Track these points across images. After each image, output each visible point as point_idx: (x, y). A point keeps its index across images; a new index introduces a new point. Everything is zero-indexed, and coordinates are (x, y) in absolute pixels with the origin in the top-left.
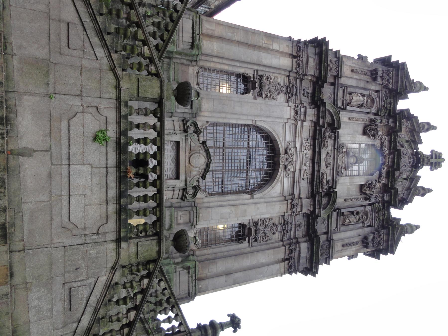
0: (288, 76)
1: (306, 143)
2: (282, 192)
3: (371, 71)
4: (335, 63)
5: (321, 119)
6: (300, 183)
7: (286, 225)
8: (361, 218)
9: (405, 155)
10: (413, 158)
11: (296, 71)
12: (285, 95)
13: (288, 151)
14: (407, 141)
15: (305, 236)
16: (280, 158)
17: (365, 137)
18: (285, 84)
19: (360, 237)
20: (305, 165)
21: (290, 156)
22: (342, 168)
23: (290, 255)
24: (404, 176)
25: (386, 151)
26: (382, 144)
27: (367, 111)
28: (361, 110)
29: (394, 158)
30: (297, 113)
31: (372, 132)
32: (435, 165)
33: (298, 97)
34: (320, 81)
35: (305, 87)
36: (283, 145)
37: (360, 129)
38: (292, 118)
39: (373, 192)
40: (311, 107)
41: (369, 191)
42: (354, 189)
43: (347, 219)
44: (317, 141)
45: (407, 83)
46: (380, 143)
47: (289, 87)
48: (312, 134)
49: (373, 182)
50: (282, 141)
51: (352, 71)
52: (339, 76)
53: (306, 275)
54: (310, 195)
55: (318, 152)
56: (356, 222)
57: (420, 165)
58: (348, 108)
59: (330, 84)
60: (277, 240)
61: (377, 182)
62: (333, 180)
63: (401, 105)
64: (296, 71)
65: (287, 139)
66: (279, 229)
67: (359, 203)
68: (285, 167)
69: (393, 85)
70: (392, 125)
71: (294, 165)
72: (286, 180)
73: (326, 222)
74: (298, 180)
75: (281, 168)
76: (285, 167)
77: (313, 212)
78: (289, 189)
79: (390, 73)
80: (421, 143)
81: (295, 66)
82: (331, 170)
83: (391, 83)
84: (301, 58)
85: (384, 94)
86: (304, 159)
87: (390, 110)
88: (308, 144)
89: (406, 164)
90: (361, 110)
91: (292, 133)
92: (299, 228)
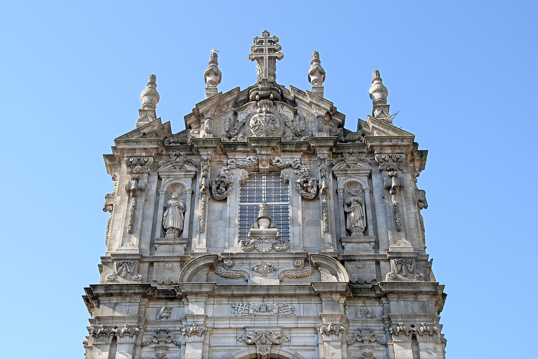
0: (142, 346)
1: (239, 310)
2: (312, 348)
3: (129, 196)
4: (121, 265)
5: (203, 290)
6: (298, 318)
7: (363, 339)
8: (357, 198)
9: (256, 123)
10: (261, 107)
11: (135, 337)
12: (171, 349)
13: (250, 341)
14: (236, 114)
15: (381, 302)
16: (261, 353)
17: (228, 200)
18: (153, 349)
19: (385, 197)
20: (271, 311)
21: (258, 337)
22: (275, 244)
23: (408, 334)
24: (290, 115)
25: (250, 159)
26: (239, 167)
27: (189, 196)
28: (188, 208)
29: (262, 147)
30: (195, 333)
31: (221, 190)
32: (275, 50)
33: (172, 326)
34: (148, 292)
35: (157, 314)
36: (242, 348)
37: (218, 206)
38: (202, 339)
39: (314, 180)
40: (185, 303)
41: (312, 187)
42: (311, 212)
43: (356, 225)
44: (235, 292)
45: (146, 131)
46: (238, 170)
47: (158, 343)
48: (225, 301)
49: (298, 181)
50: (237, 352)
51: (131, 232)
52: (139, 257)
53: (444, 296)
54: (317, 299)
55: (251, 291)
56: (362, 206)
57: (272, 96)
58: (185, 234)
59: (151, 269)
60: (385, 353)
61: (299, 172)
62: (295, 259)
63: (178, 127)
64: (135, 337)
65: (232, 341)
66: (367, 351)
67: (331, 203)
68: (274, 344)
69: (149, 154)
70: (210, 153)
71: (271, 330)
72: (296, 341)
73: (360, 264)
74: (294, 322)
75: (276, 351)
76: (274, 344)
77: (342, 294)
78: (307, 335)
79: (131, 162)
80: (239, 88)
81: (127, 339)
82: (280, 261)
83: (146, 160)
84: (116, 331)
85: (164, 167)
86: (262, 314)
87: (188, 155)
88: (240, 307)
89: (271, 121)
90: (188, 208)
91: (224, 333)
92: (369, 315)
